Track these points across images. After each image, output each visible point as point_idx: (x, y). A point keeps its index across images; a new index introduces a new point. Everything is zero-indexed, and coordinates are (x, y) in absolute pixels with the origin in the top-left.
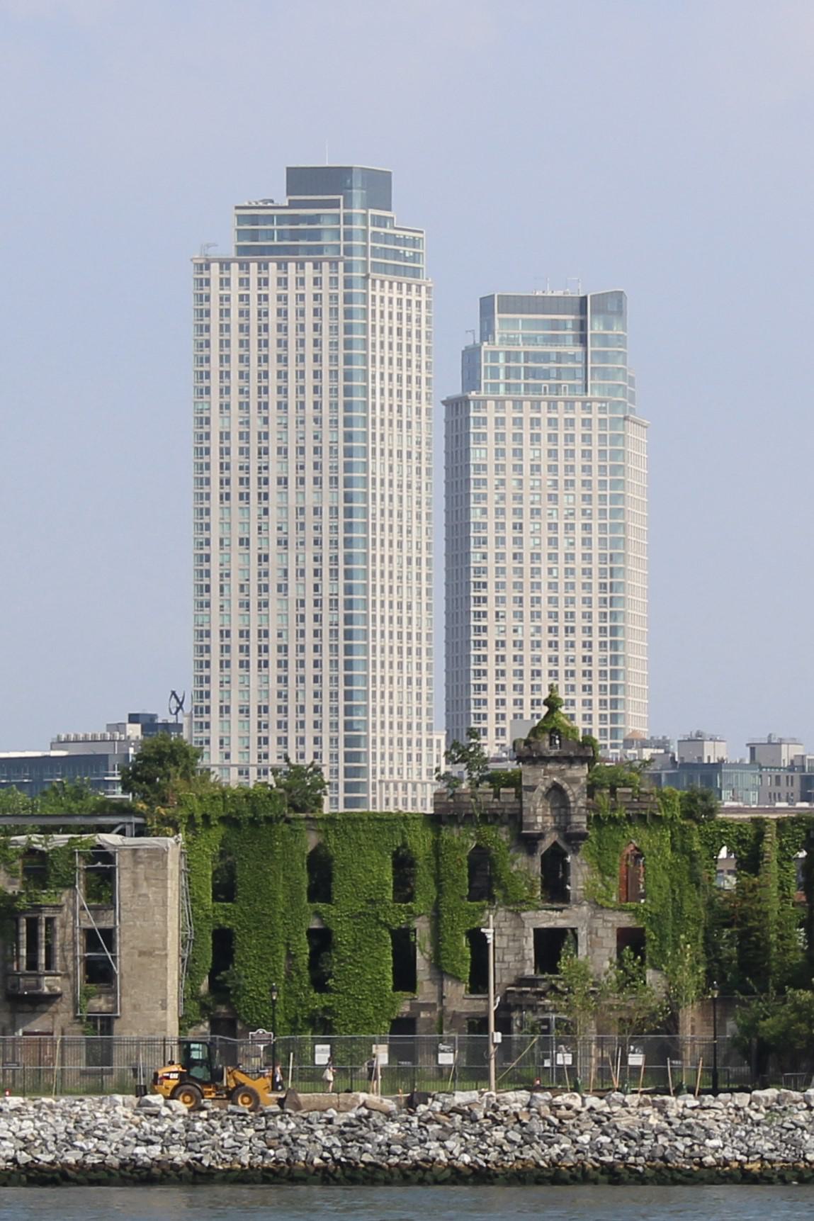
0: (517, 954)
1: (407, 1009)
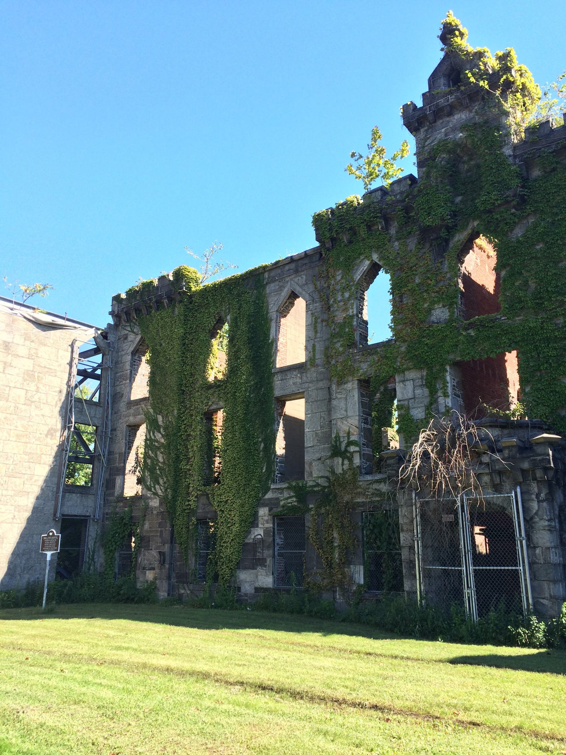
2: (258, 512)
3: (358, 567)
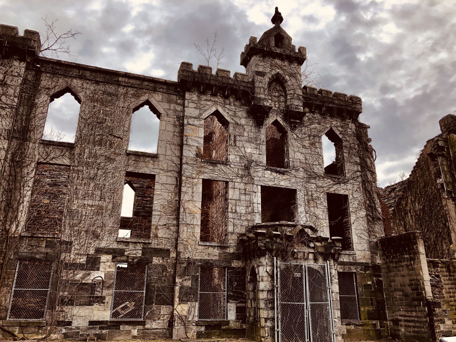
0: (247, 207)
1: (139, 254)
2: (100, 258)
3: (194, 304)
